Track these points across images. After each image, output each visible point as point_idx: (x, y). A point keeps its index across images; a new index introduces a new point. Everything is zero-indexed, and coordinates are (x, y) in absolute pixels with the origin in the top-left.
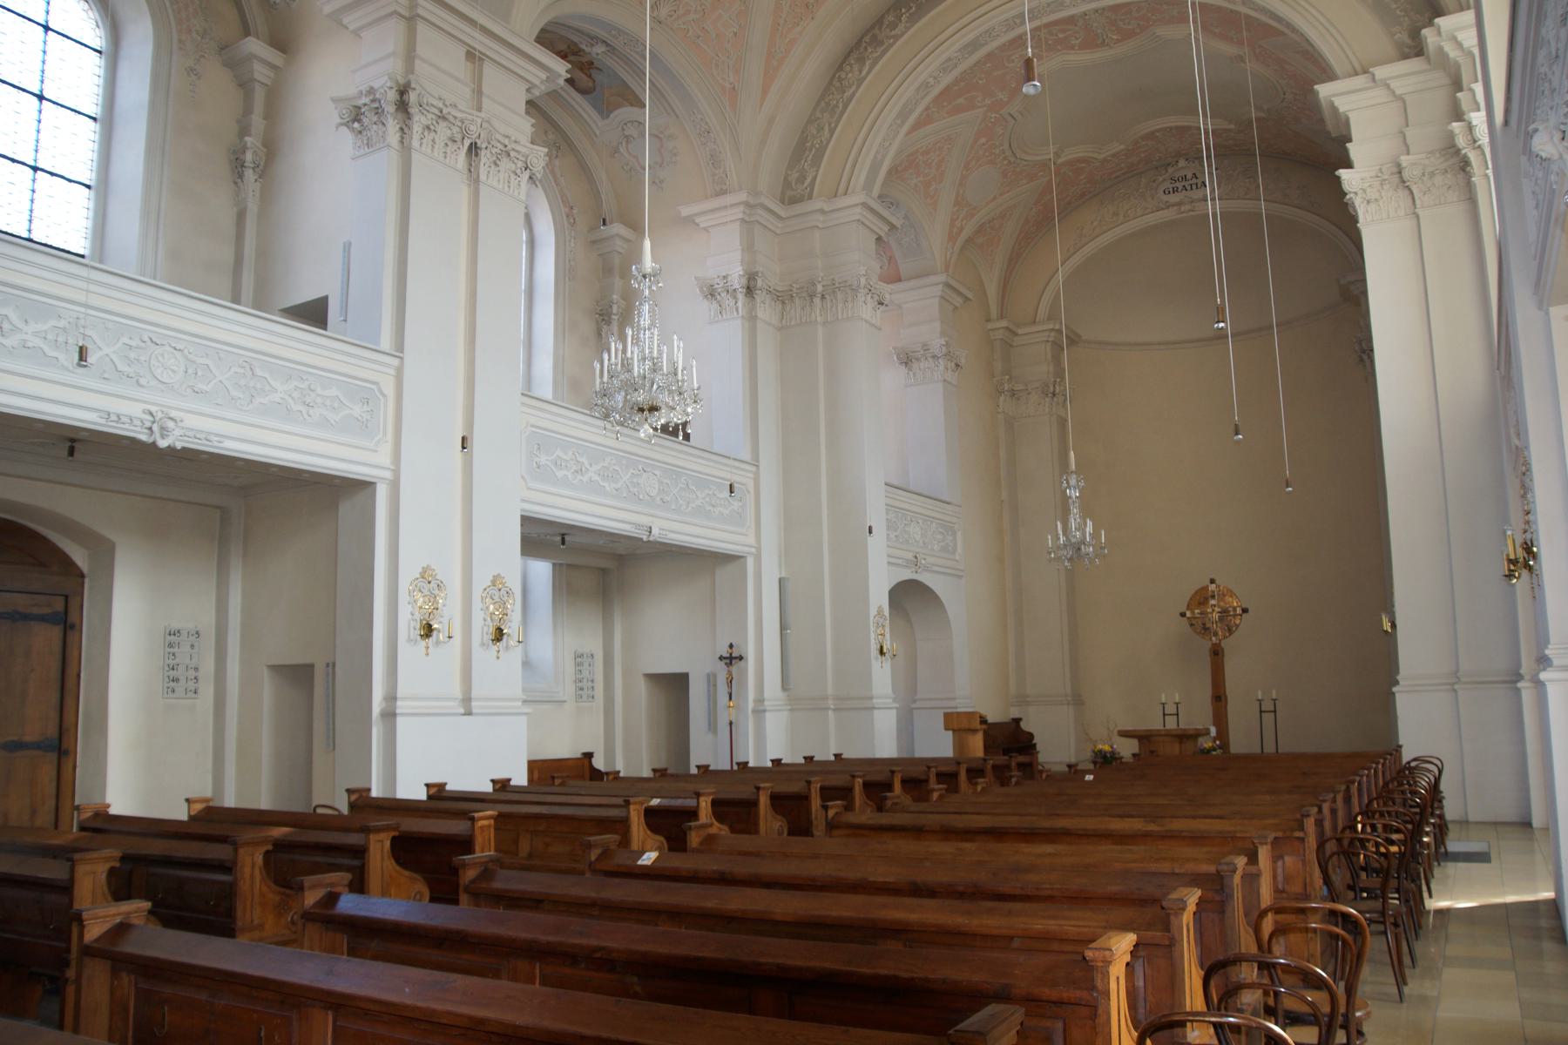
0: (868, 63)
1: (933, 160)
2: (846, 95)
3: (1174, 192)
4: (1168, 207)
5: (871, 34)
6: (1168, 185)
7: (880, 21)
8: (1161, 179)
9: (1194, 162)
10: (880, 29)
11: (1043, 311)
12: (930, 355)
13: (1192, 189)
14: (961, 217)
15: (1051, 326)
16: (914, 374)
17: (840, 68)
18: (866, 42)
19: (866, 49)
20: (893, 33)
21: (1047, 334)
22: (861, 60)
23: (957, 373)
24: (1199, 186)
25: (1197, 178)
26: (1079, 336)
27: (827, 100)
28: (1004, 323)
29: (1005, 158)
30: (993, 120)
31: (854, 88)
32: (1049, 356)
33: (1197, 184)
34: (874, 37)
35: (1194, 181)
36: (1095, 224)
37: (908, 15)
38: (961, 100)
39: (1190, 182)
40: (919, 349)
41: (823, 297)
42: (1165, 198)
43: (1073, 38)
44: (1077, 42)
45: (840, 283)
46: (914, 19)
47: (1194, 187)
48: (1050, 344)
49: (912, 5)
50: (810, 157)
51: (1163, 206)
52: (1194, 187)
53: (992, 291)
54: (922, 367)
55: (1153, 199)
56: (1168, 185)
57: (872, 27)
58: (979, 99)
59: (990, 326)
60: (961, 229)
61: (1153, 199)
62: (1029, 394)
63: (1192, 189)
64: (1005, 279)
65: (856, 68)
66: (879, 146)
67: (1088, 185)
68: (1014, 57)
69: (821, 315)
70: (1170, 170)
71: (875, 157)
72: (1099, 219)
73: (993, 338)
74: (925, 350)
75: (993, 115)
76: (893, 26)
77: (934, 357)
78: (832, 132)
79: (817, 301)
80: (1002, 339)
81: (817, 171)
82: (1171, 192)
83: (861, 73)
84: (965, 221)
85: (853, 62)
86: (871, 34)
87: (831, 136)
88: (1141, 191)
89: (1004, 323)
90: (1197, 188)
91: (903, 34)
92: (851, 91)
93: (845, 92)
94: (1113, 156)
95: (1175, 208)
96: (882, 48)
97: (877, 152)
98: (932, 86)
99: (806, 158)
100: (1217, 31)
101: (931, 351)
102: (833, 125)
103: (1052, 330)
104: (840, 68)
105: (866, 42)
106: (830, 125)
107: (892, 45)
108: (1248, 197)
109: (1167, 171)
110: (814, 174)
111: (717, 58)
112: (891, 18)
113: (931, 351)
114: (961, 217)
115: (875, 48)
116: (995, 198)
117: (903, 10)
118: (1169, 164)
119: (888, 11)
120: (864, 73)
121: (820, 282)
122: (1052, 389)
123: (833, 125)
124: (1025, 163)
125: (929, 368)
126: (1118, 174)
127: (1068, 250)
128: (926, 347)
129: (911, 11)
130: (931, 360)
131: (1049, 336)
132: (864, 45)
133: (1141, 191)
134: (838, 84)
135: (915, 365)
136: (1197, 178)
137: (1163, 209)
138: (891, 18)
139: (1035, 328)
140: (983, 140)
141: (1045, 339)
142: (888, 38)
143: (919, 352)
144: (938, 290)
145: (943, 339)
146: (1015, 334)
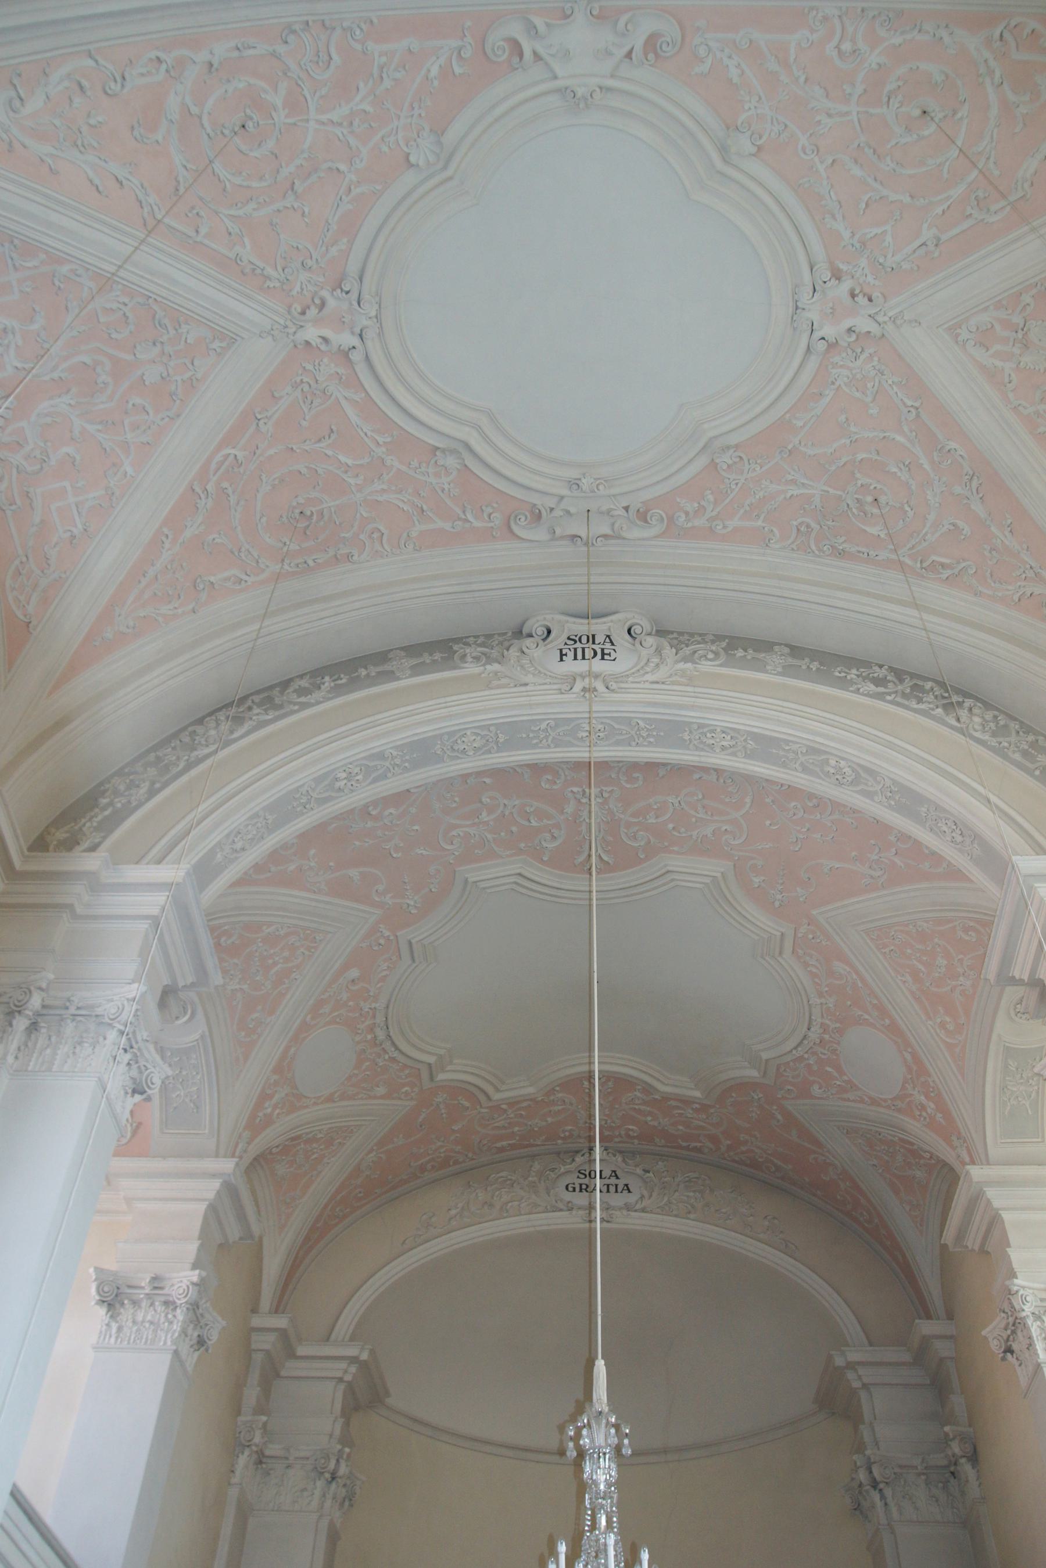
0: (247, 726)
1: (275, 964)
2: (196, 753)
3: (581, 1191)
4: (570, 1209)
5: (266, 694)
6: (573, 1179)
7: (285, 684)
8: (562, 1170)
9: (615, 1156)
10: (282, 693)
11: (345, 1325)
12: (163, 1299)
13: (608, 1191)
14: (277, 1097)
15: (352, 1351)
16: (120, 1329)
17: (200, 721)
18: (253, 702)
19: (250, 709)
20: (303, 699)
21: (343, 1365)
22: (238, 720)
23: (197, 1354)
24: (619, 1190)
25: (617, 1178)
26: (387, 1394)
27: (160, 754)
28: (281, 1322)
29: (371, 1029)
30: (382, 941)
31: (213, 748)
32: (338, 1406)
33: (616, 1186)
34: (270, 699)
35: (613, 1181)
36: (453, 1212)
37: (332, 684)
38: (354, 873)
39: (607, 1181)
40: (143, 1284)
41: (33, 1027)
42: (568, 1196)
43: (548, 836)
44: (551, 845)
45: (78, 1008)
46: (338, 690)
47: (612, 1189)
48: (342, 1387)
49: (342, 676)
50: (100, 818)
51: (560, 1205)
52: (612, 1189)
53: (273, 1267)
54: (140, 1317)
55: (548, 1194)
56: (573, 1179)
57: (271, 688)
58: (381, 888)
59: (256, 1321)
60: (268, 1121)
61: (548, 1194)
62: (288, 1467)
63: (608, 1191)
64: (294, 1261)
65: (225, 727)
66: (228, 836)
67: (458, 1148)
68: (454, 833)
69: (16, 1058)
70: (579, 1159)
71: (212, 852)
72: (460, 1205)
73: (253, 1346)
74: (156, 1288)
75: (387, 933)
76: (302, 692)
77: (166, 1303)
78: (152, 793)
79: (21, 1024)
80: (267, 1352)
81: (105, 838)
82: (578, 1189)
83: (232, 732)
84: (277, 1111)
85: (223, 718)
86: (266, 694)
87: (148, 800)
88: (530, 1179)
89: (281, 1322)
90: (616, 1191)
91: (318, 703)
92: (207, 751)
93: (193, 749)
94: (511, 1105)
95: (581, 1212)
96: (277, 713)
97: (219, 845)
98: (340, 790)
99: (92, 817)
100: (756, 880)
101: (165, 1292)
102: (158, 785)
103: (353, 1360)
104: (200, 721)
105: (253, 702)
106: (153, 783)
107: (296, 712)
108: (692, 1216)
109: (573, 1160)
110: (97, 841)
111: (24, 559)
112: (304, 683)
113: (165, 1292)
114: (277, 1097)
115: (266, 710)
116: (330, 1099)
117: (327, 678)
118: (577, 1152)
119: (301, 677)
120: (236, 735)
121: (40, 989)
122: (332, 1465)
123: (158, 785)
124: (396, 1054)
125: (151, 1323)
126: (504, 1143)
127: (404, 1242)
128: (157, 1281)
129: (340, 682)
130: (160, 1308)
131: (346, 1371)
132: (249, 703)
133: (530, 1179)
134: (187, 740)
135: (127, 1313)
136: (617, 1178)
137: (561, 1210)
138: (304, 683)
139: (328, 1351)
140: (354, 973)
141: (339, 1374)
142: (290, 703)
143: (143, 1288)
144: (211, 1188)
145: (197, 1272)
146: (292, 1355)
